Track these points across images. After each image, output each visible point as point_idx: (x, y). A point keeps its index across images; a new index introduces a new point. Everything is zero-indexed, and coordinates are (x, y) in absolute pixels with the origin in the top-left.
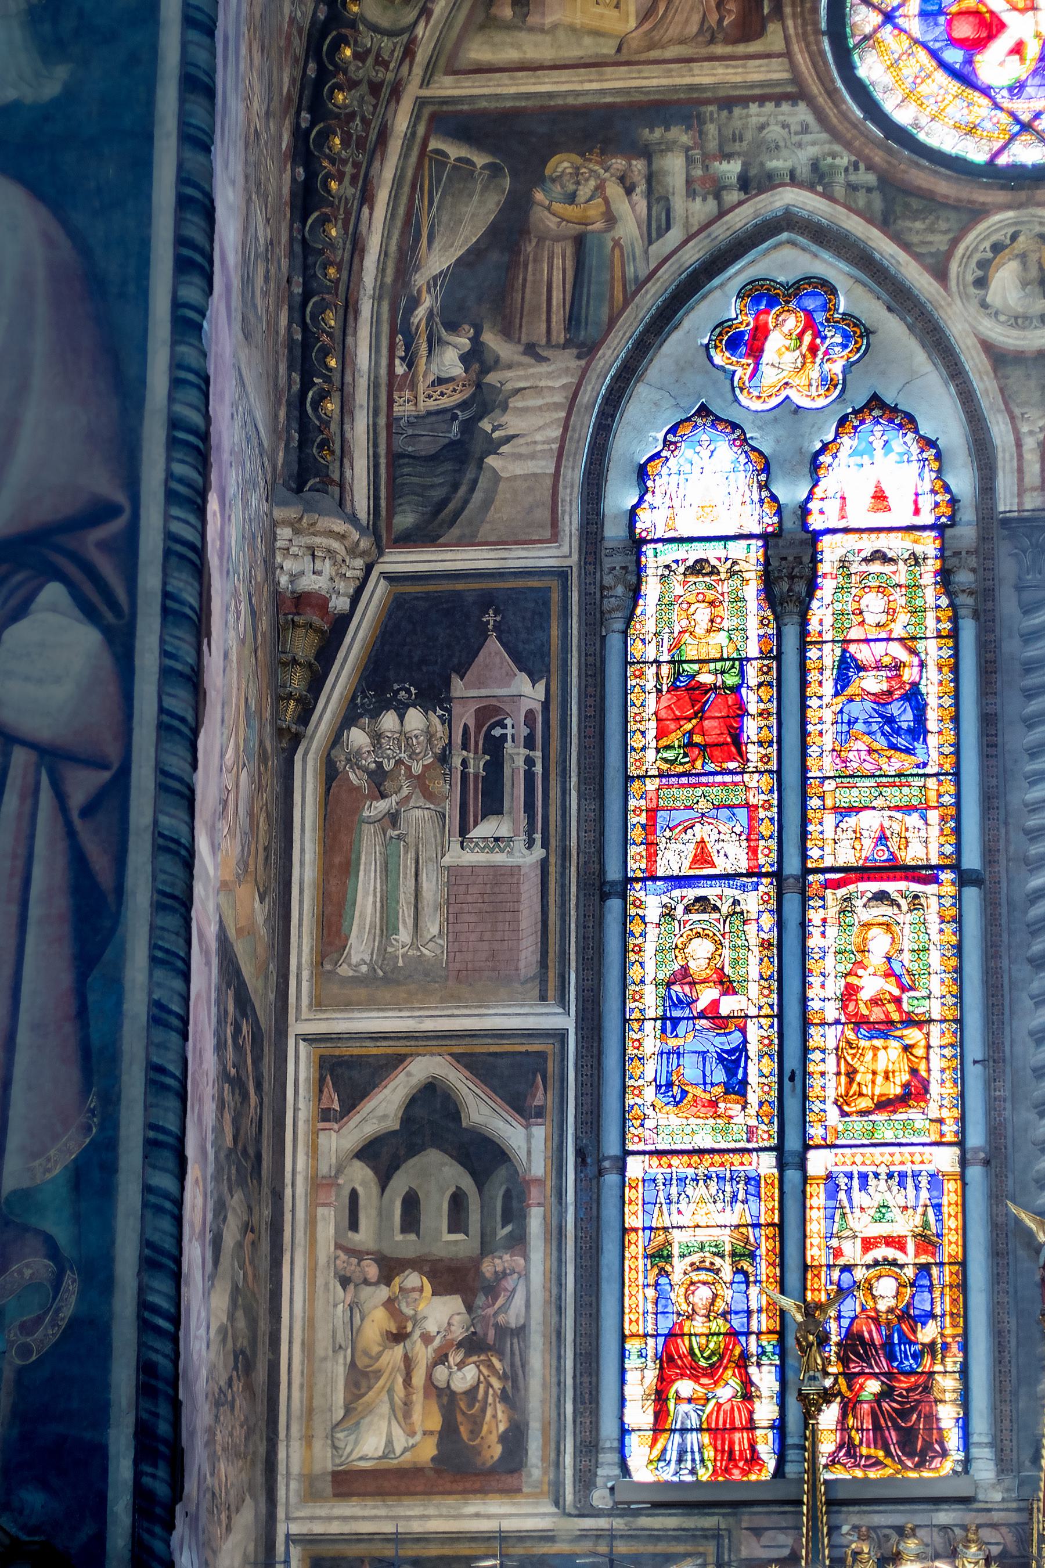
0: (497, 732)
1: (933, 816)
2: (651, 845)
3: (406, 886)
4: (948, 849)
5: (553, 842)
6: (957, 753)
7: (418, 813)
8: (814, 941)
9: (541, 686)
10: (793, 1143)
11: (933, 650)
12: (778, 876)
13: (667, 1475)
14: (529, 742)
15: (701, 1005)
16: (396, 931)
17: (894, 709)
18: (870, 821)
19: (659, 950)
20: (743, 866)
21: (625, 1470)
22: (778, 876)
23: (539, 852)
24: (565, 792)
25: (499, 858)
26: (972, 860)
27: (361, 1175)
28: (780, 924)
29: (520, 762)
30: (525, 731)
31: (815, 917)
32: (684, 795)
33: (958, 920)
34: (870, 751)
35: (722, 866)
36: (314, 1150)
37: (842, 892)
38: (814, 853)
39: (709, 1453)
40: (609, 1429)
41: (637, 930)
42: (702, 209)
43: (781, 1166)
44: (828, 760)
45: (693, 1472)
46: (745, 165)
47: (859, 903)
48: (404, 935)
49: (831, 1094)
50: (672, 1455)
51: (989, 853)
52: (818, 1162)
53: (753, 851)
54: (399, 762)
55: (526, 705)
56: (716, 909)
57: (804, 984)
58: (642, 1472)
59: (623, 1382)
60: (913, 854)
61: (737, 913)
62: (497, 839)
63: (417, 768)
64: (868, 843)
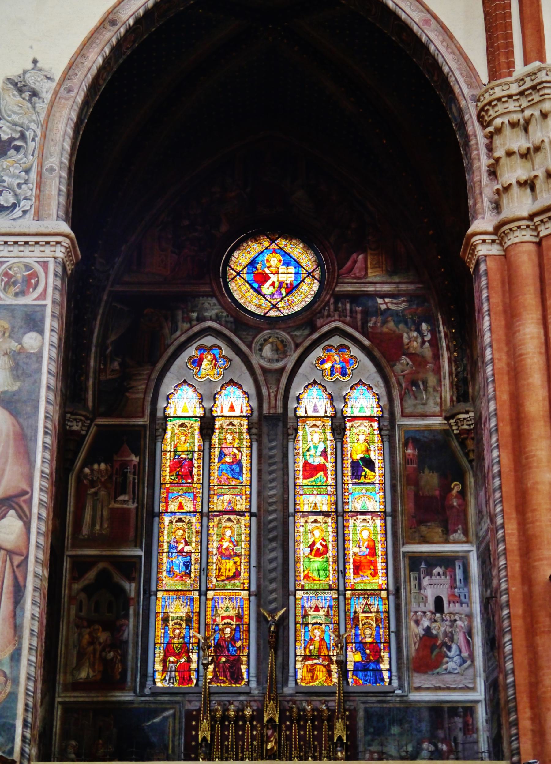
0: (126, 470)
1: (244, 497)
2: (167, 502)
3: (99, 513)
4: (248, 507)
5: (140, 502)
6: (251, 480)
7: (103, 493)
8: (211, 532)
9: (138, 458)
10: (203, 588)
11: (245, 451)
12: (201, 513)
13: (166, 685)
14: (134, 474)
15: (179, 549)
16: (95, 526)
17: (234, 467)
18: (226, 498)
19: (168, 533)
20: (192, 510)
21: (154, 683)
22: (201, 513)
23: (135, 505)
24: (143, 488)
25: (125, 506)
26: (254, 510)
27: (83, 596)
28: (201, 526)
29: (131, 479)
30: (133, 470)
31: (211, 525)
32: (176, 489)
33: (250, 526)
34: (227, 478)
35: (186, 509)
36: (70, 589)
37: (218, 518)
38: (211, 506)
39: (178, 678)
40: (150, 670)
41: (162, 527)
42: (186, 326)
43: (200, 595)
44: (216, 480)
45: (173, 683)
46: (198, 314)
47: (223, 521)
48: (98, 527)
49: (214, 575)
50: (167, 678)
51: (259, 508)
52: (210, 594)
53: (194, 505)
54: (98, 478)
55: (134, 463)
56: (184, 522)
57: (208, 544)
58: (159, 685)
59: (154, 657)
60: (238, 508)
61: (189, 522)
62: (124, 501)
63: (103, 479)
64: (226, 504)
